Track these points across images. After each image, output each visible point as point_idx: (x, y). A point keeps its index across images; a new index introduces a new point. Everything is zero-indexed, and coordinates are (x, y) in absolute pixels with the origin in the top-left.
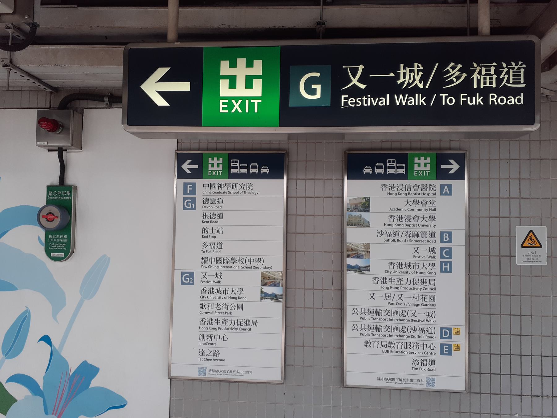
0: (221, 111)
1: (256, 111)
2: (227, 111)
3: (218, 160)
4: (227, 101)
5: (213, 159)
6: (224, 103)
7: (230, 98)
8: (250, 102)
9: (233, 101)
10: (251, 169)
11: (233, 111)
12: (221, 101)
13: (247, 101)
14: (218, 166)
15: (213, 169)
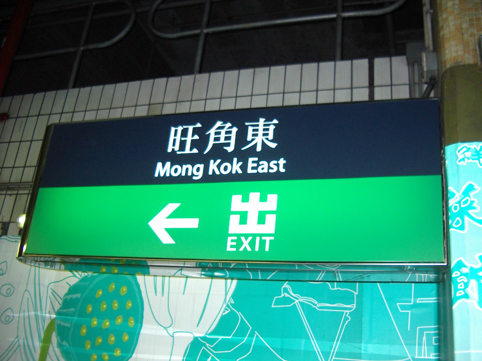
0: (229, 249)
1: (267, 249)
2: (234, 249)
4: (235, 238)
6: (232, 241)
7: (239, 236)
8: (261, 239)
9: (243, 238)
11: (241, 249)
12: (230, 239)
13: (258, 239)
14: (261, 220)
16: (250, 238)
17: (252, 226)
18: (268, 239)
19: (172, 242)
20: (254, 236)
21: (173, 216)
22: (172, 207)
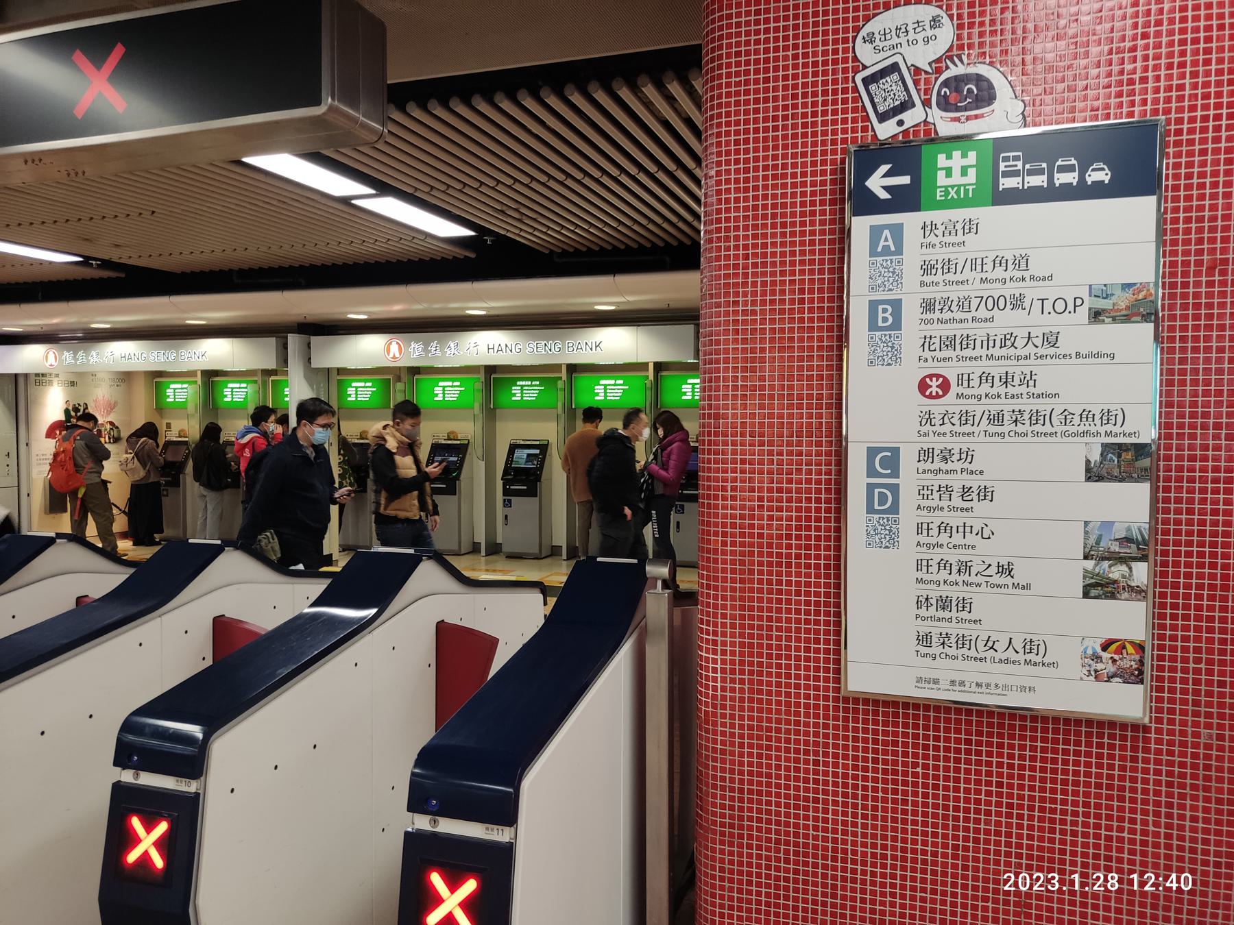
5: (949, 157)
15: (949, 182)
17: (957, 179)
18: (971, 188)
20: (959, 186)
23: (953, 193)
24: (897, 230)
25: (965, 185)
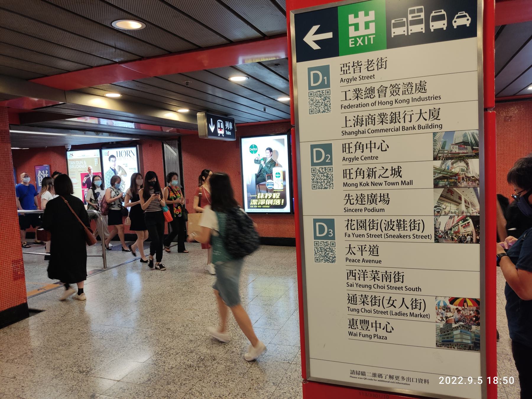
3: (367, 14)
5: (356, 16)
10: (431, 24)
14: (367, 26)
16: (362, 38)
17: (362, 31)
18: (372, 37)
19: (319, 48)
20: (364, 36)
21: (317, 33)
22: (315, 28)
23: (360, 41)
24: (325, 70)
25: (368, 35)
